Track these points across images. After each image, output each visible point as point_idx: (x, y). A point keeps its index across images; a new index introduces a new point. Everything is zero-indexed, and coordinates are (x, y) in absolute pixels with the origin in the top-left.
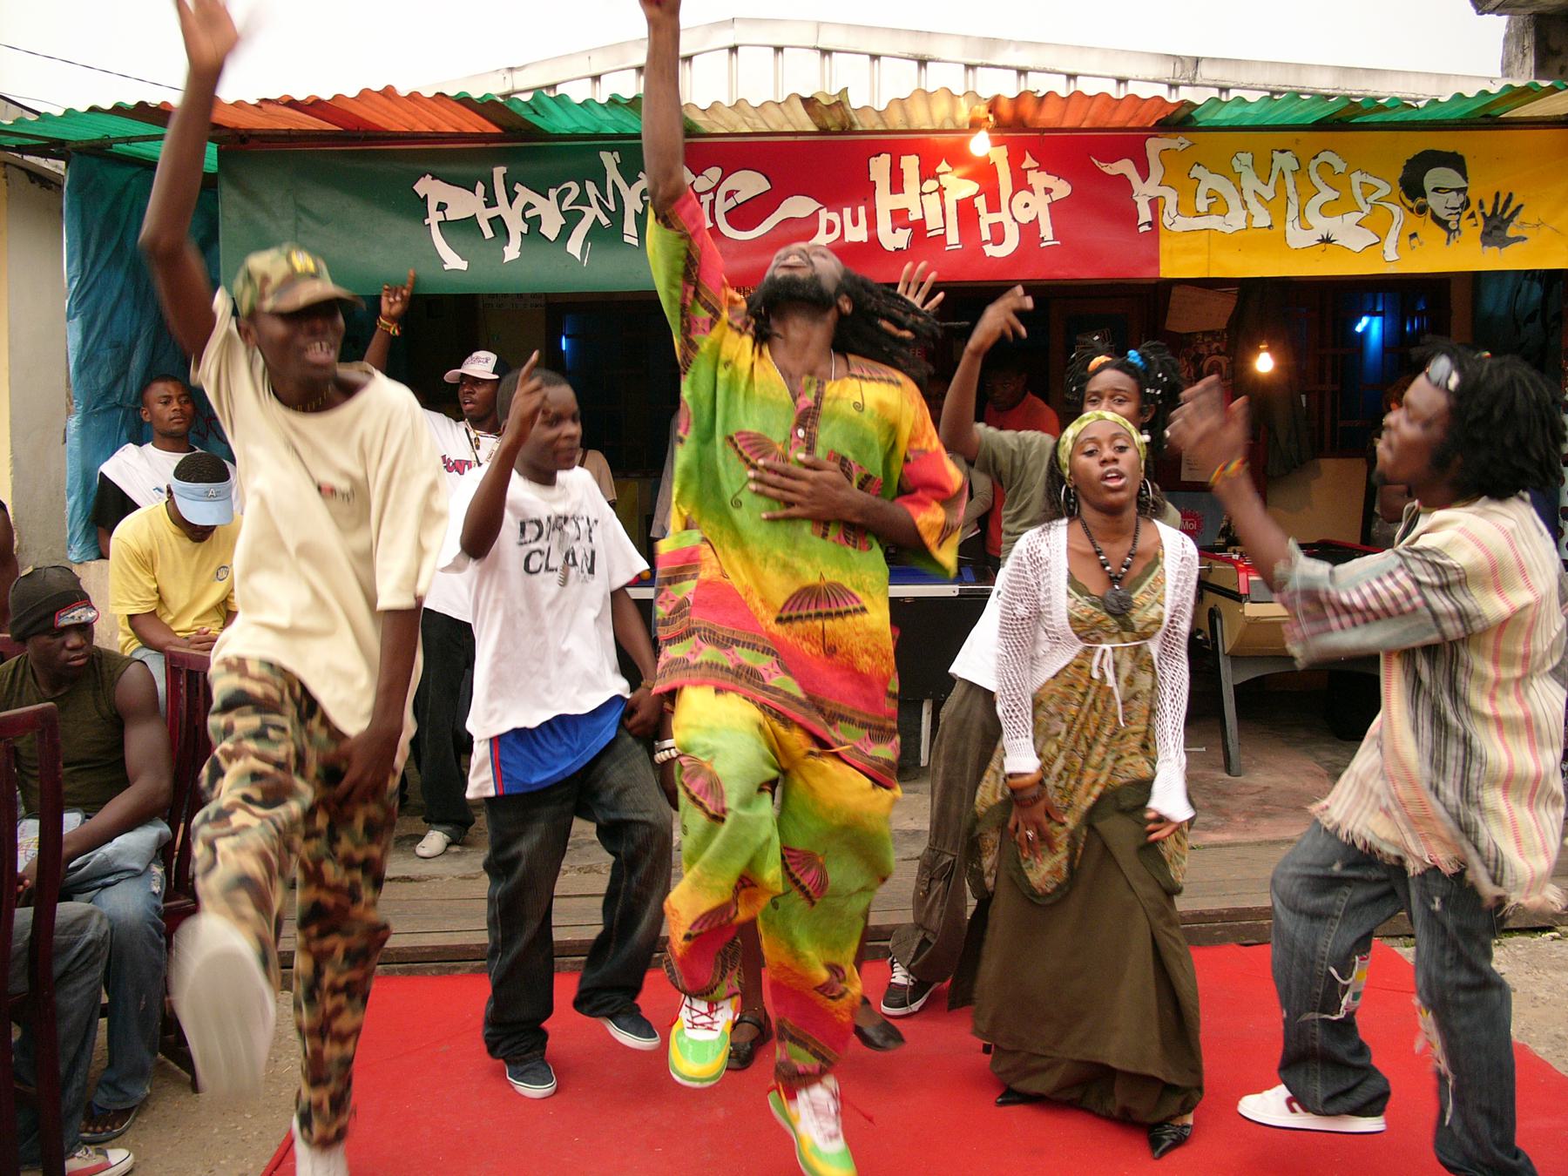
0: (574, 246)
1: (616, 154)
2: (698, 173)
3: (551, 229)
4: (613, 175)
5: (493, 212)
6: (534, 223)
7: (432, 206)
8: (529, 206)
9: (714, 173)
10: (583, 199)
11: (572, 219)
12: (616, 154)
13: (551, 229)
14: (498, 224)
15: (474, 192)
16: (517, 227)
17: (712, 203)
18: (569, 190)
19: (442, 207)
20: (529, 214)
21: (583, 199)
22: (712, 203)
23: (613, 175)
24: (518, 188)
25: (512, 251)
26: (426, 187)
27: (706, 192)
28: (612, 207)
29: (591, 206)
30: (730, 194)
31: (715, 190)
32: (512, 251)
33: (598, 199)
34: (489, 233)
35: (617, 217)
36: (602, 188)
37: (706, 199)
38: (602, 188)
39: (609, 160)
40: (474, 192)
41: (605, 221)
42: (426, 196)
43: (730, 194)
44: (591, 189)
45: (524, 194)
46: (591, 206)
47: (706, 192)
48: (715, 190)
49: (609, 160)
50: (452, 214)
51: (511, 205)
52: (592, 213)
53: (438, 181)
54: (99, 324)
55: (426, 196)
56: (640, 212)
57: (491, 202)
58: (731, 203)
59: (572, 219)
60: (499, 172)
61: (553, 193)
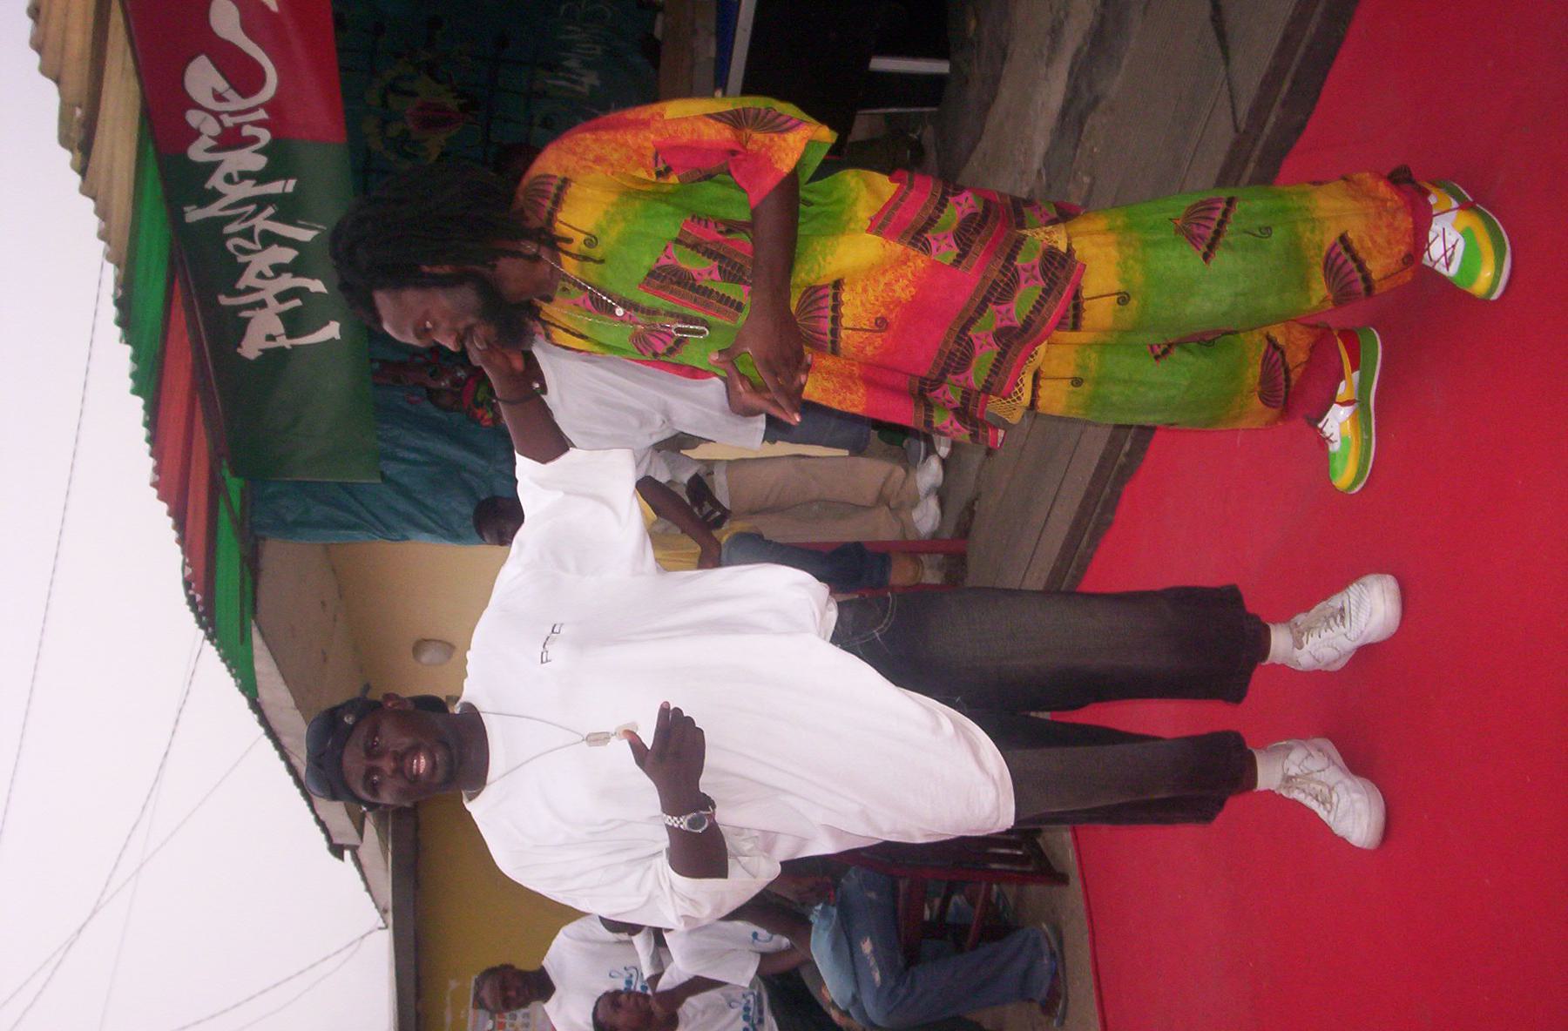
0: (306, 235)
1: (186, 209)
2: (196, 134)
3: (287, 255)
4: (213, 210)
5: (272, 302)
6: (278, 269)
7: (272, 345)
8: (261, 275)
9: (193, 118)
10: (248, 234)
11: (269, 239)
12: (186, 209)
13: (288, 255)
14: (282, 297)
15: (251, 318)
16: (287, 281)
17: (233, 114)
18: (239, 249)
19: (271, 338)
20: (271, 274)
21: (248, 234)
22: (233, 114)
23: (213, 210)
24: (241, 285)
25: (317, 286)
26: (252, 347)
27: (220, 122)
28: (252, 208)
29: (251, 229)
30: (219, 97)
31: (216, 115)
32: (317, 286)
33: (243, 221)
34: (297, 303)
35: (262, 202)
36: (230, 220)
37: (229, 122)
38: (230, 220)
39: (194, 215)
40: (251, 318)
41: (270, 211)
42: (260, 350)
43: (219, 97)
44: (231, 228)
45: (249, 279)
46: (254, 226)
47: (220, 122)
48: (216, 115)
49: (194, 215)
50: (278, 327)
51: (262, 290)
52: (261, 223)
53: (243, 343)
54: (411, 510)
55: (260, 350)
56: (253, 182)
57: (262, 304)
58: (231, 94)
59: (269, 239)
60: (224, 300)
61: (242, 259)
